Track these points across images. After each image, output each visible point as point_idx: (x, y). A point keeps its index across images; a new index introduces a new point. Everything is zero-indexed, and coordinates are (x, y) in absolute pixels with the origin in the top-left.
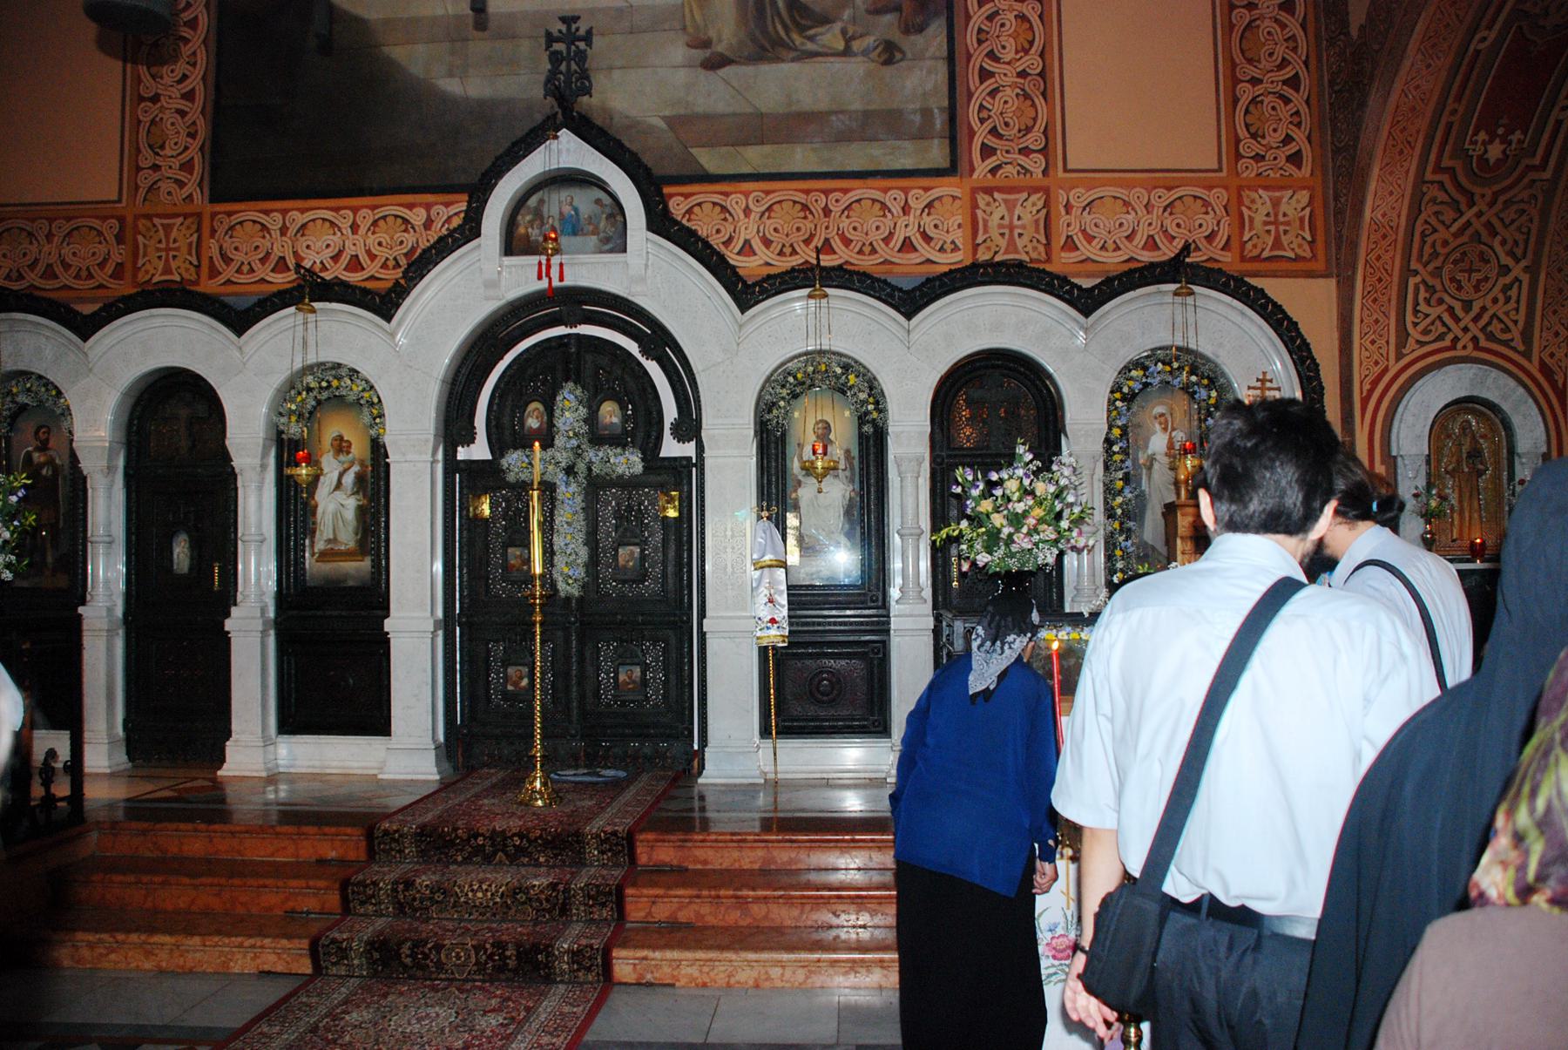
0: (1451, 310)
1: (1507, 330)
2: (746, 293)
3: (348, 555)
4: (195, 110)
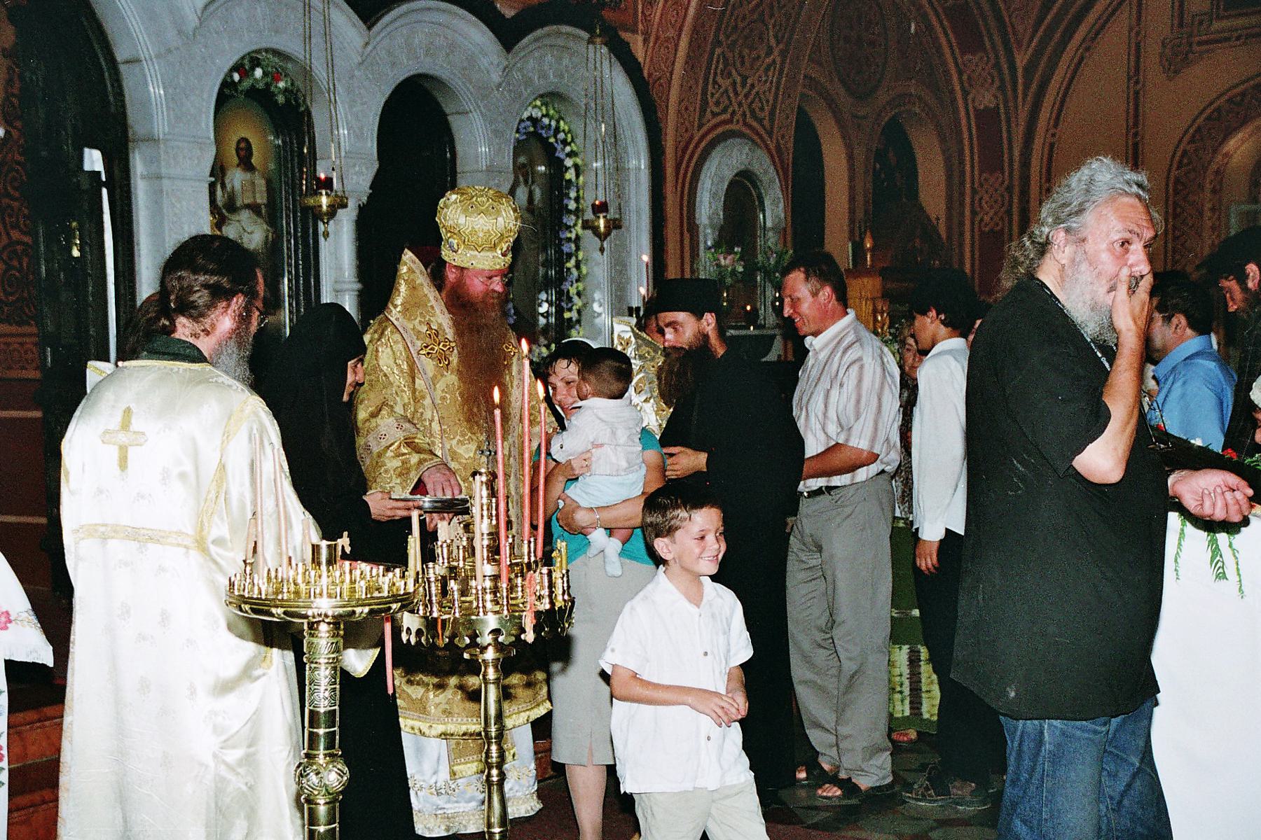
0: (734, 83)
1: (762, 109)
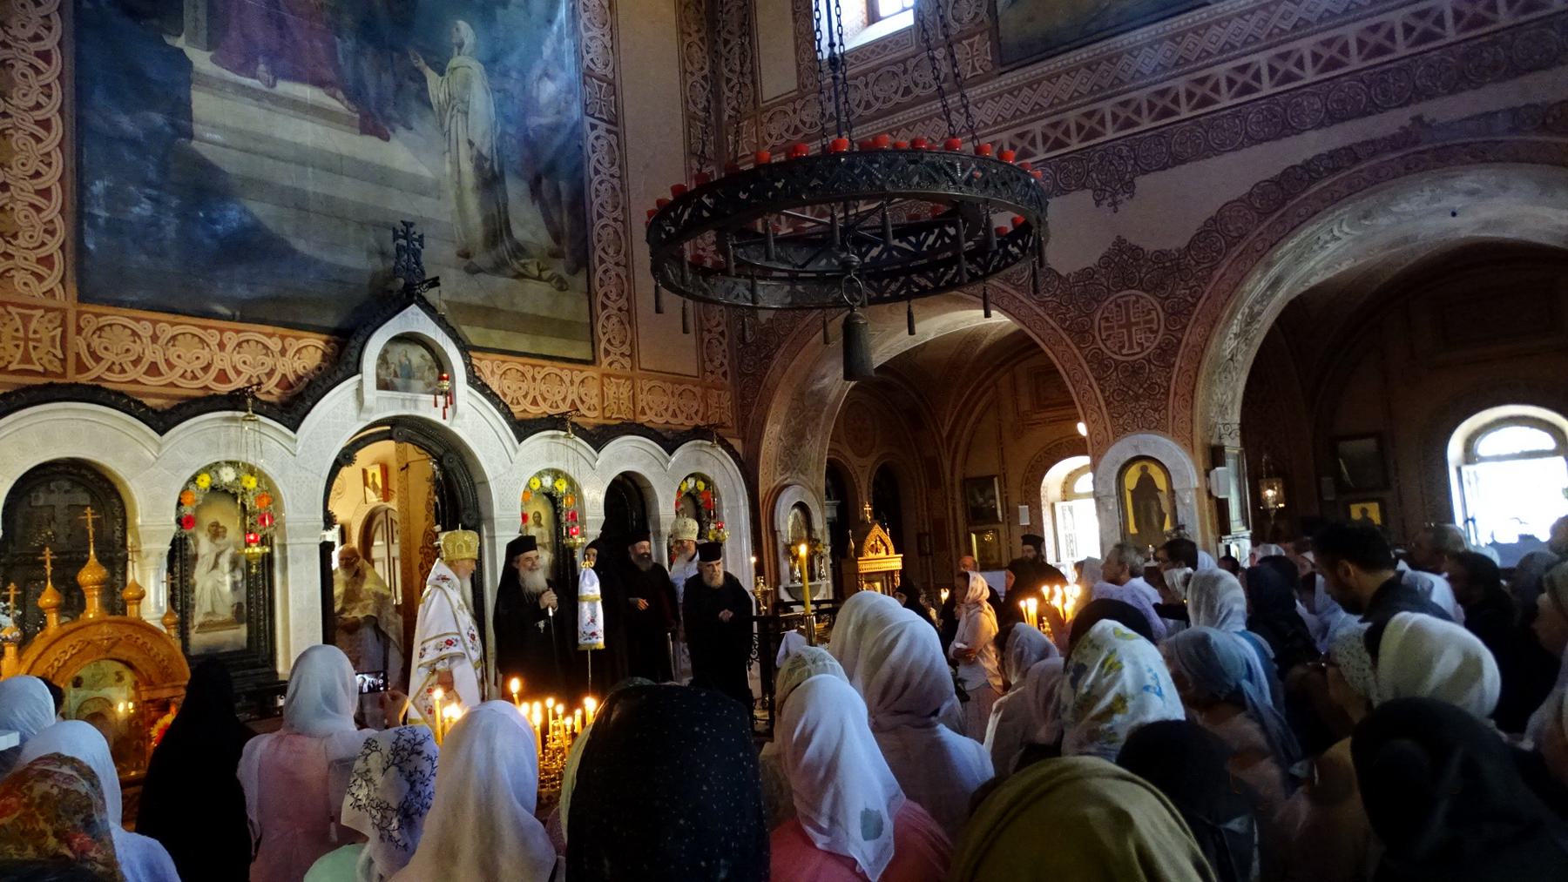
2: (523, 428)
3: (224, 625)
4: (52, 210)
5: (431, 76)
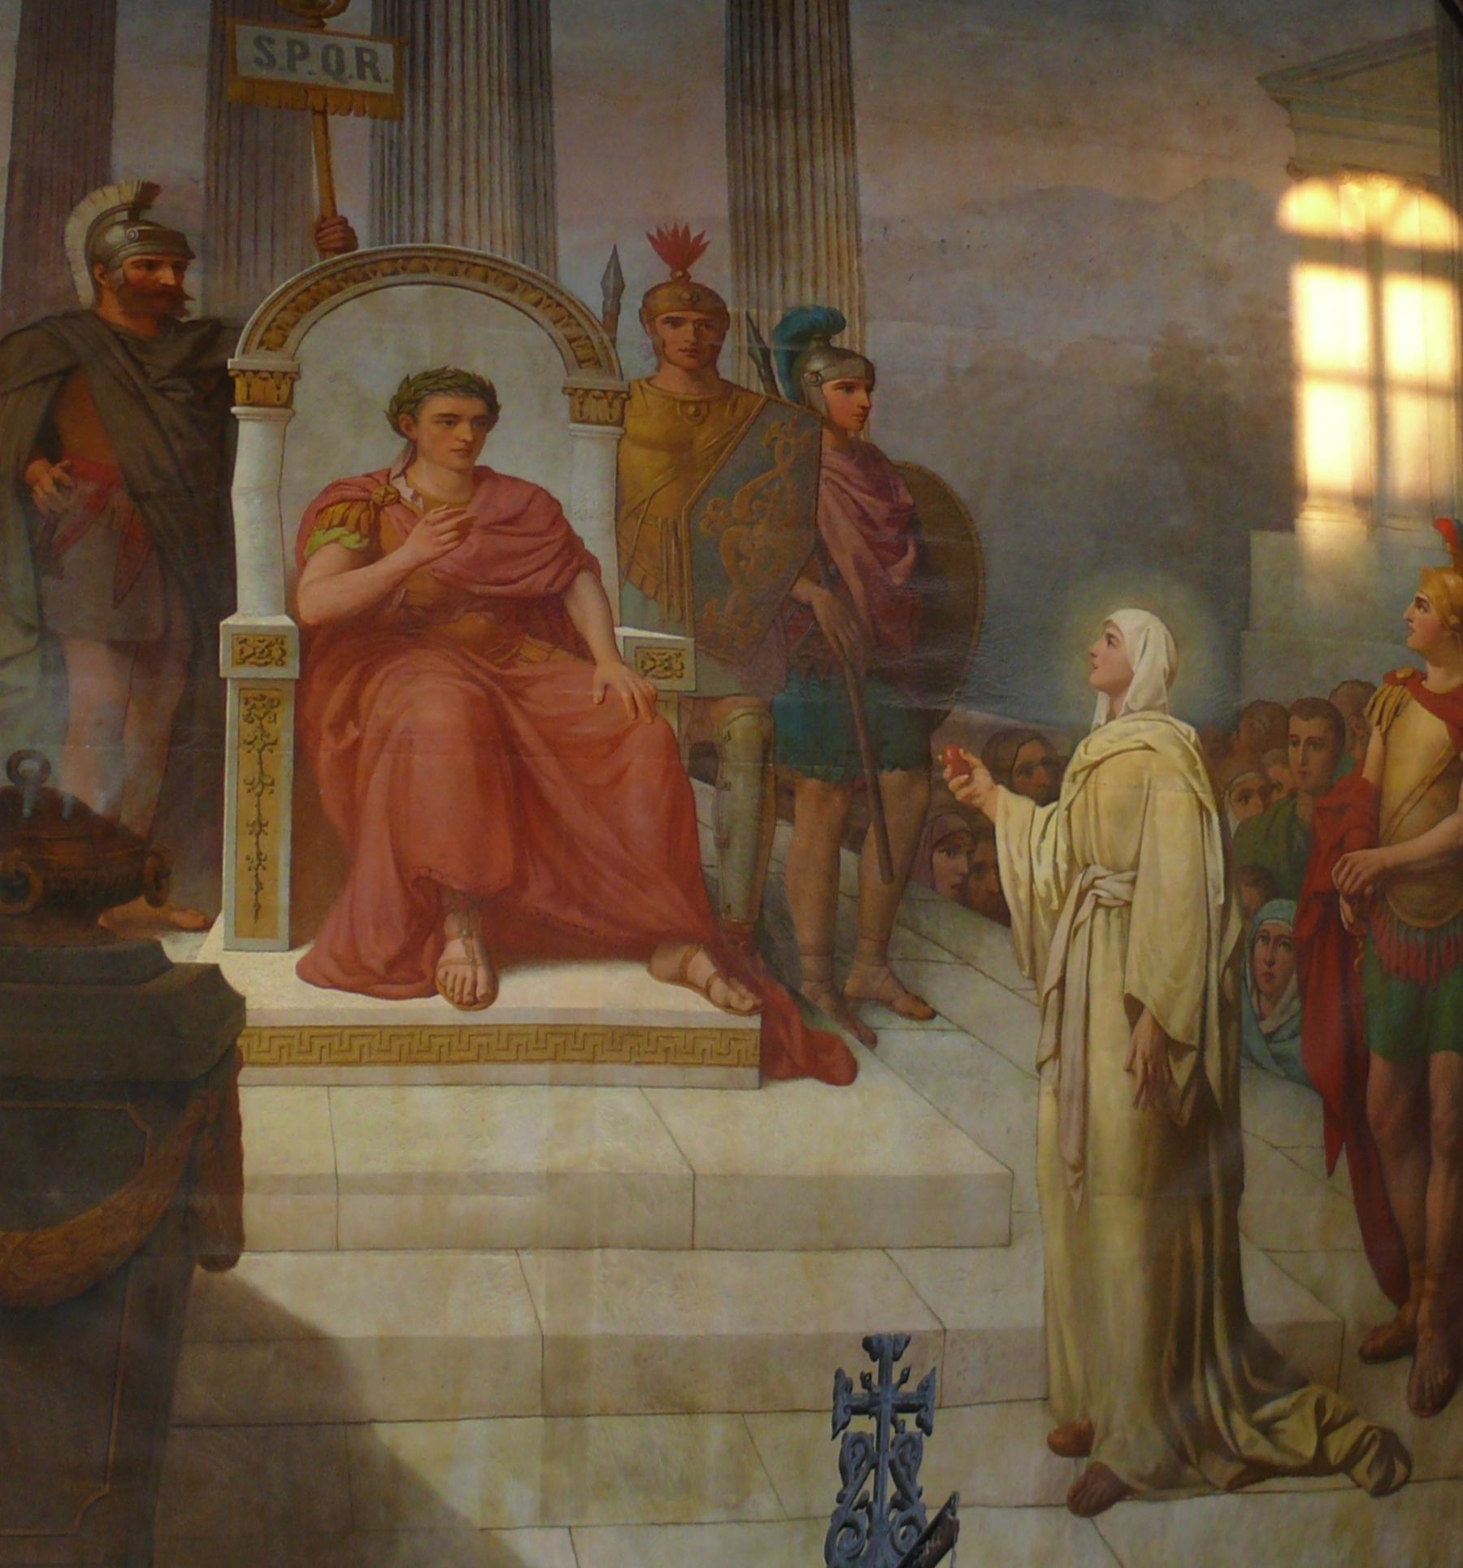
5: (1012, 815)
